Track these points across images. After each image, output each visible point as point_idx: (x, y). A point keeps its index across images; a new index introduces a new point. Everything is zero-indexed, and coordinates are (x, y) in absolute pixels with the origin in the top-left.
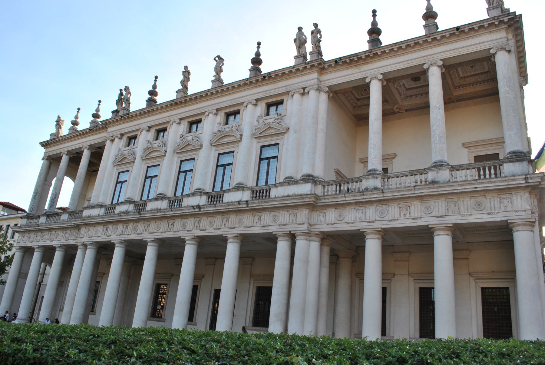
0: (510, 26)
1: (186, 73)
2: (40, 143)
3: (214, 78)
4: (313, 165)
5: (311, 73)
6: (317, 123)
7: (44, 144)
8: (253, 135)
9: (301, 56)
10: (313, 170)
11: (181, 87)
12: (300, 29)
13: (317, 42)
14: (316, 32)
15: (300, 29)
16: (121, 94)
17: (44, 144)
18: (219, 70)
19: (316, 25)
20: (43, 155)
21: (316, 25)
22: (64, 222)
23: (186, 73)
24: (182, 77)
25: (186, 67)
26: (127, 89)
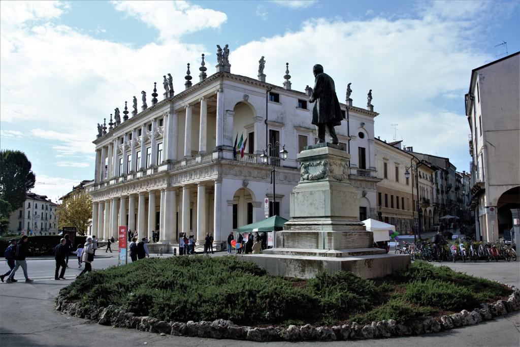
0: (223, 76)
1: (135, 100)
2: (93, 142)
3: (143, 105)
4: (170, 154)
5: (168, 104)
6: (172, 132)
7: (95, 142)
8: (155, 138)
9: (166, 94)
10: (170, 157)
11: (134, 109)
12: (165, 77)
13: (171, 84)
14: (171, 78)
15: (165, 77)
16: (116, 113)
17: (95, 142)
18: (144, 99)
19: (169, 75)
20: (95, 149)
21: (169, 75)
22: (106, 187)
23: (135, 100)
24: (133, 104)
25: (134, 97)
26: (117, 109)
